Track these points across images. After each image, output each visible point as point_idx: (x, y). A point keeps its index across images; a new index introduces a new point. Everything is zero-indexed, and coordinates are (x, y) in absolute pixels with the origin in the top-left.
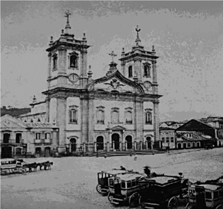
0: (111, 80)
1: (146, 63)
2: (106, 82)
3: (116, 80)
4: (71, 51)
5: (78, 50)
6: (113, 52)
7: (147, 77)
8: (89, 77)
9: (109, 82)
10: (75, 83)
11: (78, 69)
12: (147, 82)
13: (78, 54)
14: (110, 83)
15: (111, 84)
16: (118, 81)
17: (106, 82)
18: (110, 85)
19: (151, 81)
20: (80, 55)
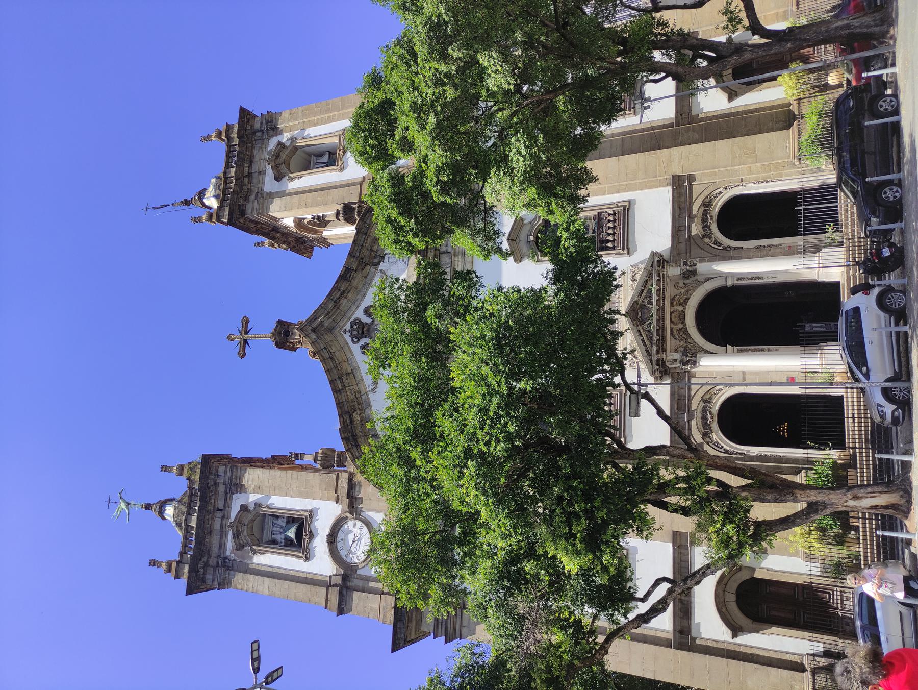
0: (356, 348)
1: (275, 168)
2: (368, 380)
11: (312, 513)
13: (244, 508)
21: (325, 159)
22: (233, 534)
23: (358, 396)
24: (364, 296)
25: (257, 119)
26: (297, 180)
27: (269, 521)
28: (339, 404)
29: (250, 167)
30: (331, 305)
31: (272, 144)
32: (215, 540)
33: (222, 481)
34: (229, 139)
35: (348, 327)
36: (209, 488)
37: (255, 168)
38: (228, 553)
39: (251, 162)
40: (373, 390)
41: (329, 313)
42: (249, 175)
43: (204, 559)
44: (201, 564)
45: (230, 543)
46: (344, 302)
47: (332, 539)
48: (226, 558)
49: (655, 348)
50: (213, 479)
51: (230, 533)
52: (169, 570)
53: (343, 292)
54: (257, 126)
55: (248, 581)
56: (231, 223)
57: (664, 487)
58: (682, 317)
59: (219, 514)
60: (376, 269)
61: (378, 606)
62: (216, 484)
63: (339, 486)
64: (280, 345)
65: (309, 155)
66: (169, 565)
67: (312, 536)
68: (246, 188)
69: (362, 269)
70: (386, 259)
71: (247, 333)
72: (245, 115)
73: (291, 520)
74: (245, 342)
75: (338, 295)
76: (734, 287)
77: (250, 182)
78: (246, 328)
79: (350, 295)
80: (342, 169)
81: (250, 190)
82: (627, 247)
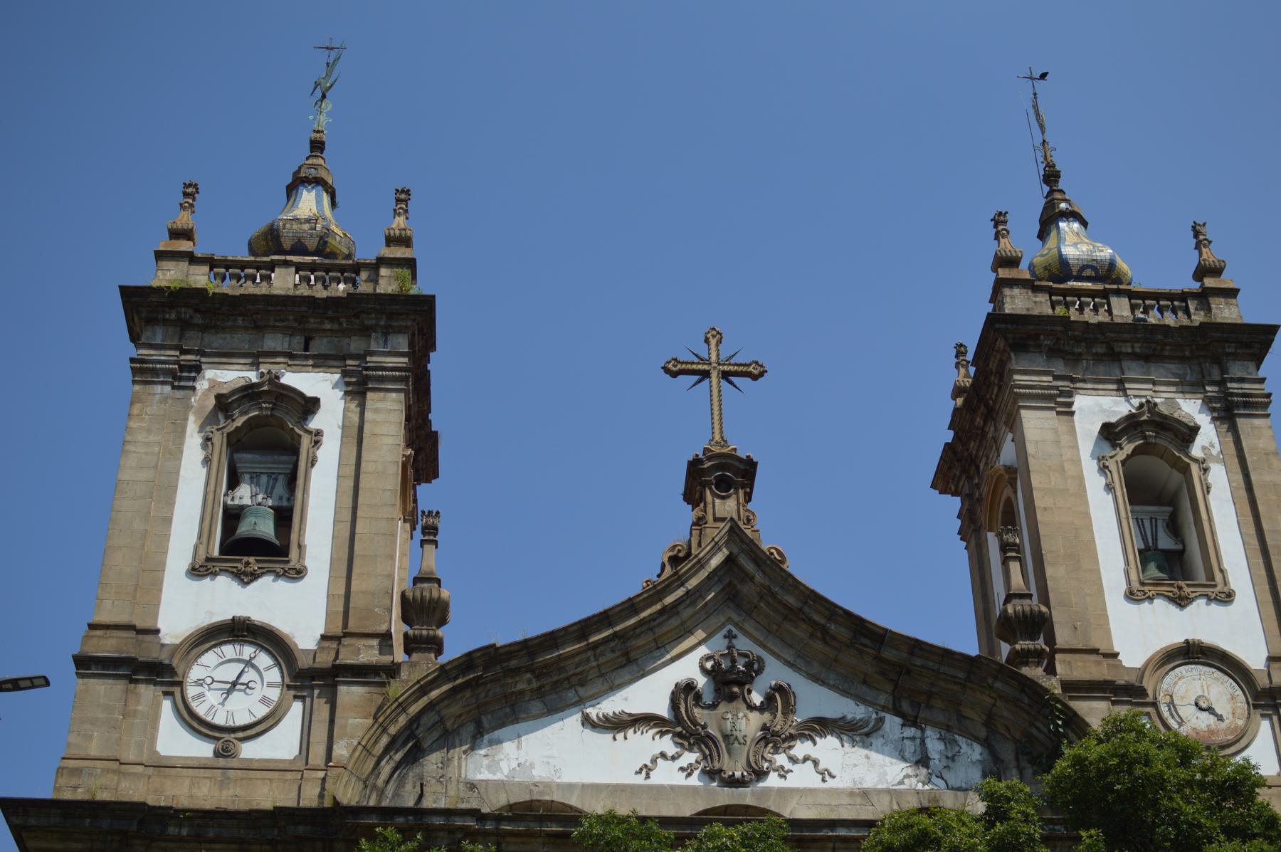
1: (1130, 425)
2: (611, 705)
4: (231, 376)
5: (321, 362)
7: (1181, 601)
8: (411, 645)
9: (650, 693)
10: (250, 751)
12: (1192, 653)
13: (312, 405)
14: (663, 710)
15: (681, 723)
16: (775, 672)
17: (611, 705)
18: (667, 744)
20: (332, 414)
21: (1166, 542)
22: (252, 386)
23: (574, 680)
24: (816, 679)
25: (1252, 366)
26: (1102, 481)
27: (279, 463)
28: (552, 639)
29: (1134, 356)
30: (791, 600)
31: (1191, 408)
32: (240, 340)
33: (373, 347)
34: (1204, 296)
35: (743, 643)
36: (357, 316)
37: (1133, 370)
38: (210, 373)
41: (774, 595)
42: (1114, 356)
43: (198, 320)
44: (186, 313)
45: (231, 376)
46: (801, 632)
48: (198, 369)
50: (381, 326)
51: (253, 376)
52: (176, 234)
53: (824, 630)
54: (1236, 370)
55: (149, 431)
56: (997, 323)
59: (298, 341)
60: (884, 709)
61: (94, 752)
62: (366, 332)
63: (361, 643)
64: (695, 468)
66: (187, 234)
67: (246, 577)
68: (1080, 349)
69: (883, 674)
70: (911, 731)
71: (725, 375)
72: (1255, 341)
73: (285, 517)
74: (705, 375)
75: (817, 618)
77: (1099, 358)
78: (737, 374)
79: (818, 645)
80: (1131, 596)
81: (1073, 359)
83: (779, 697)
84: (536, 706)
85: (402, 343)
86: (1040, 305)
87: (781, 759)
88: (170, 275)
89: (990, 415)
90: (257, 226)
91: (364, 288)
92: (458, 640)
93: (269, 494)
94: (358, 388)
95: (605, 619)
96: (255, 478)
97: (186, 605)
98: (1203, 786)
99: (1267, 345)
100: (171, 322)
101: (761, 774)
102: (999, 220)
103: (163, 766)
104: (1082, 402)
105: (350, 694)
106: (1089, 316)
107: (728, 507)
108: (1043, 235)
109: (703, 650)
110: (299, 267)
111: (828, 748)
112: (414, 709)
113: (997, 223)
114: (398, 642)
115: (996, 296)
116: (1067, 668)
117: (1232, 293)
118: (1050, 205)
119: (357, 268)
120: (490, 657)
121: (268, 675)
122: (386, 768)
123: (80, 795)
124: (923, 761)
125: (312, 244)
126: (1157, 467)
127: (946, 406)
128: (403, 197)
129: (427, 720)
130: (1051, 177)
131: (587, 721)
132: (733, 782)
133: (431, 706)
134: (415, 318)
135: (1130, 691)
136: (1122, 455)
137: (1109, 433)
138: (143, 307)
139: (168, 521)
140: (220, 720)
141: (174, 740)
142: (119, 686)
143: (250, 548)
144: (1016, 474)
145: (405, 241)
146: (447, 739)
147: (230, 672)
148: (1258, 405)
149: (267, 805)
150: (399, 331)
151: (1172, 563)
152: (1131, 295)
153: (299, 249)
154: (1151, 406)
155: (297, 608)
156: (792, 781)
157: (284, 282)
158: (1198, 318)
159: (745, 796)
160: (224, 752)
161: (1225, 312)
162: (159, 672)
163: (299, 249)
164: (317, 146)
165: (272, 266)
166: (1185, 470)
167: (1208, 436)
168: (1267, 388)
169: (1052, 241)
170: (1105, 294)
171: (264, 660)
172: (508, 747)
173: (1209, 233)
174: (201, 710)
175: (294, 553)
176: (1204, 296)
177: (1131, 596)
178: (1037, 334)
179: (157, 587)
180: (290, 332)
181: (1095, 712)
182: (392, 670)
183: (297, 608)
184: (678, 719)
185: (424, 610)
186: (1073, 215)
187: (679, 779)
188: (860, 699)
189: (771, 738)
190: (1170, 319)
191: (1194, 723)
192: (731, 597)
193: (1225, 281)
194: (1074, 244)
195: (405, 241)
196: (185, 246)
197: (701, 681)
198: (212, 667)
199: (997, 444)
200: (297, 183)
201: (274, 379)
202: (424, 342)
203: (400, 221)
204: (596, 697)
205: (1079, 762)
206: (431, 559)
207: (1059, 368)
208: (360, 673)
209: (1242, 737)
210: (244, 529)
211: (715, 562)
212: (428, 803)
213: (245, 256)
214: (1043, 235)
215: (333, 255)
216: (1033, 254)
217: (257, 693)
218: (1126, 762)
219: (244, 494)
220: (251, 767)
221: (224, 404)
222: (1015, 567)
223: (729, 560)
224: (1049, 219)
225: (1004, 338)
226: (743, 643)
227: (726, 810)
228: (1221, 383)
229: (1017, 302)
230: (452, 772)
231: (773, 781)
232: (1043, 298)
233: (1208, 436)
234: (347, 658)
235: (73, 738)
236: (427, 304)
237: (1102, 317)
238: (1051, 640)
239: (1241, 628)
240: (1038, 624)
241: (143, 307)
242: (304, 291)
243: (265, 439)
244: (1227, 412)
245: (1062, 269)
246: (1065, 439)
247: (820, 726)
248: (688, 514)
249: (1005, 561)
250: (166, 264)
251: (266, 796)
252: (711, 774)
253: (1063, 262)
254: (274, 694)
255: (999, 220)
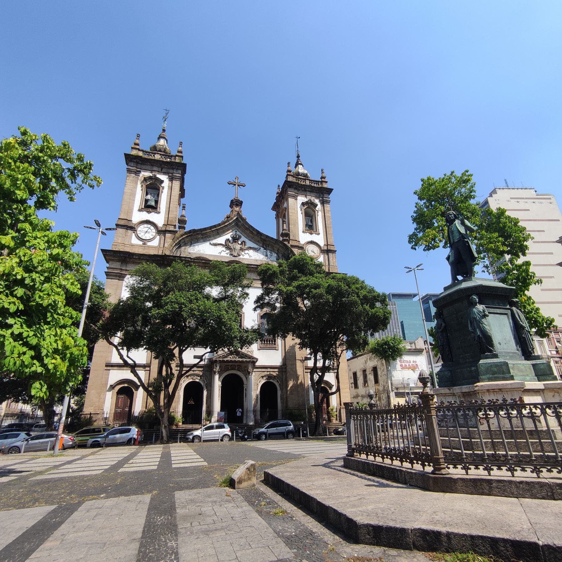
2: (215, 241)
3: (240, 237)
4: (147, 174)
5: (165, 173)
6: (237, 178)
7: (311, 234)
8: (180, 227)
9: (221, 240)
10: (149, 244)
12: (312, 242)
13: (162, 182)
14: (224, 243)
15: (226, 246)
16: (243, 238)
18: (224, 249)
19: (322, 243)
21: (310, 224)
24: (250, 240)
27: (156, 192)
28: (205, 229)
29: (309, 191)
31: (317, 201)
32: (149, 167)
34: (322, 182)
37: (308, 193)
39: (311, 192)
40: (210, 244)
42: (305, 191)
45: (147, 174)
46: (248, 232)
47: (148, 222)
48: (140, 172)
49: (221, 359)
50: (176, 168)
51: (151, 175)
52: (136, 144)
54: (325, 196)
56: (286, 182)
57: (169, 366)
58: (232, 369)
59: (160, 169)
62: (173, 169)
64: (232, 201)
65: (312, 217)
66: (138, 145)
67: (149, 212)
71: (238, 185)
72: (329, 191)
73: (157, 202)
74: (235, 185)
76: (243, 388)
77: (303, 191)
80: (303, 232)
81: (299, 190)
82: (260, 349)
83: (243, 243)
84: (202, 240)
85: (180, 172)
86: (294, 180)
87: (243, 253)
88: (134, 152)
89: (283, 198)
90: (152, 145)
91: (173, 160)
92: (188, 227)
93: (154, 197)
94: (171, 179)
95: (215, 226)
96: (151, 194)
97: (137, 216)
98: (314, 265)
99: (331, 192)
100: (135, 162)
101: (239, 255)
102: (289, 163)
103: (133, 245)
104: (299, 198)
105: (168, 235)
106: (302, 183)
107: (237, 209)
108: (295, 167)
109: (231, 233)
110: (160, 155)
111: (251, 252)
112: (180, 239)
113: (288, 164)
114: (177, 227)
115: (287, 177)
116: (291, 243)
117: (327, 182)
118: (297, 162)
119: (172, 156)
120: (194, 231)
121: (153, 230)
122: (175, 249)
123: (117, 250)
124: (267, 256)
125: (163, 150)
126: (310, 211)
127: (276, 195)
128: (181, 143)
129: (182, 241)
130: (298, 157)
131: (210, 244)
132: (235, 256)
133: (183, 239)
134: (182, 167)
135: (301, 248)
136: (305, 208)
137: (303, 204)
138: (129, 158)
139: (134, 200)
140: (144, 238)
141: (135, 241)
142: (124, 230)
143: (149, 207)
144: (287, 209)
145: (181, 152)
146: (185, 245)
147: (146, 229)
148: (328, 202)
149: (152, 254)
150: (179, 169)
151: (310, 227)
152: (310, 180)
153: (160, 151)
154: (311, 200)
155: (159, 219)
156: (245, 257)
157: (157, 157)
158: (320, 186)
159: (236, 259)
160: (144, 244)
161: (325, 185)
162: (132, 228)
163: (160, 151)
164: (164, 130)
165: (155, 154)
166: (315, 212)
167: (319, 207)
168: (330, 199)
169: (297, 169)
170: (305, 179)
171: (152, 228)
172: (196, 247)
173: (324, 171)
174: (140, 236)
175: (158, 209)
176: (322, 182)
177: (303, 232)
178: (293, 185)
179: (132, 212)
180: (158, 167)
181: (296, 251)
182: (176, 232)
183: (159, 219)
184: (226, 245)
185: (182, 222)
186: (301, 164)
187: (226, 255)
188: (257, 244)
189: (241, 249)
190: (315, 185)
191: (310, 254)
192: (237, 225)
193: (326, 180)
194: (301, 169)
195: (181, 152)
196: (137, 147)
197: (230, 239)
198: (142, 229)
199: (284, 203)
200: (160, 137)
201: (155, 176)
202: (184, 172)
203: (180, 148)
204: (212, 240)
205: (295, 259)
206: (184, 213)
207: (296, 191)
208: (170, 232)
209: (318, 257)
210: (149, 203)
211: (234, 218)
212: (182, 256)
213: (149, 151)
214: (295, 167)
215: (167, 153)
216: (294, 170)
217: (151, 233)
218: (303, 260)
219: (149, 197)
220: (149, 247)
221: (145, 179)
222: (285, 225)
223: (237, 218)
224: (297, 165)
225: (288, 185)
226: (238, 233)
227: (233, 261)
228: (323, 198)
229: (290, 179)
230: (186, 251)
231: (241, 257)
232: (295, 179)
233: (319, 207)
234: (168, 229)
235: (115, 239)
236: (185, 165)
237: (304, 183)
238: (289, 238)
239: (320, 239)
240: (287, 235)
241: (129, 158)
242: (161, 159)
243: (153, 187)
244: (323, 203)
245: (298, 174)
246: (296, 204)
247: (250, 248)
248: (230, 209)
249: (283, 224)
250: (134, 150)
251: (152, 252)
252: (231, 255)
253: (299, 173)
254: (154, 234)
255: (289, 163)
